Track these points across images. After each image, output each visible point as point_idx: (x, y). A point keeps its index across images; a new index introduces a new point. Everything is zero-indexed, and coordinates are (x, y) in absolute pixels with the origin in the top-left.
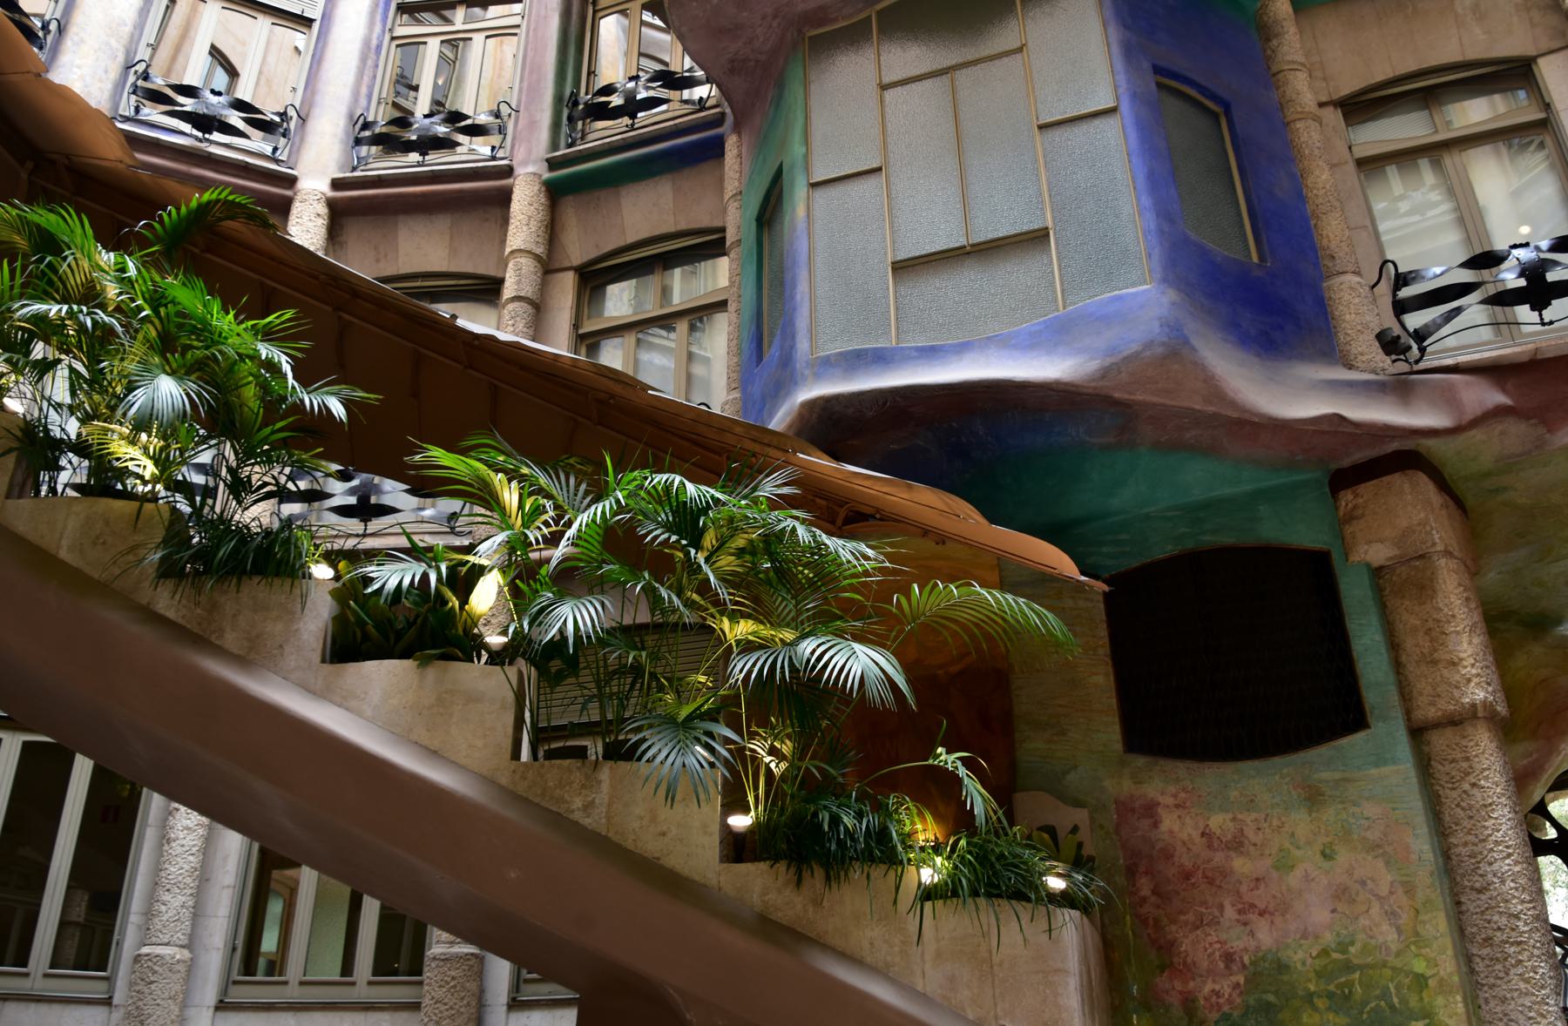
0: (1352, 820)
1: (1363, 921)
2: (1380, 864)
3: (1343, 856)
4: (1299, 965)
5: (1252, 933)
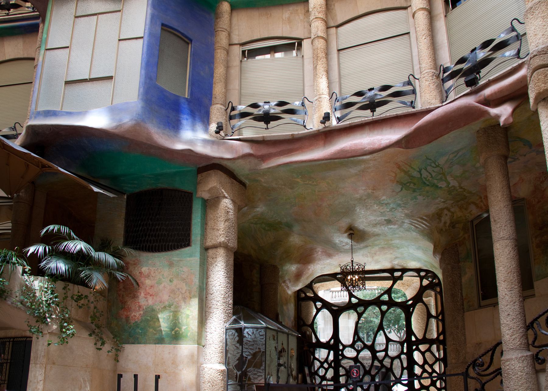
1: (177, 299)
2: (184, 284)
3: (175, 281)
5: (147, 301)
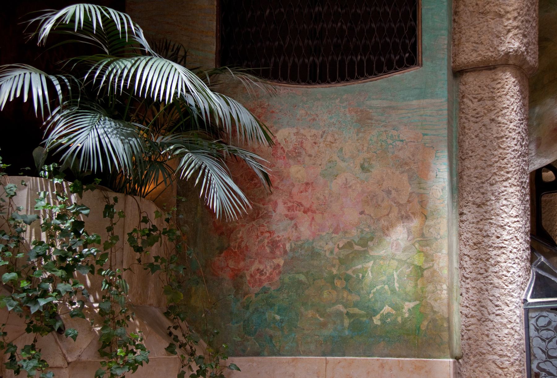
0: (390, 141)
3: (377, 170)
4: (327, 254)
5: (296, 226)
